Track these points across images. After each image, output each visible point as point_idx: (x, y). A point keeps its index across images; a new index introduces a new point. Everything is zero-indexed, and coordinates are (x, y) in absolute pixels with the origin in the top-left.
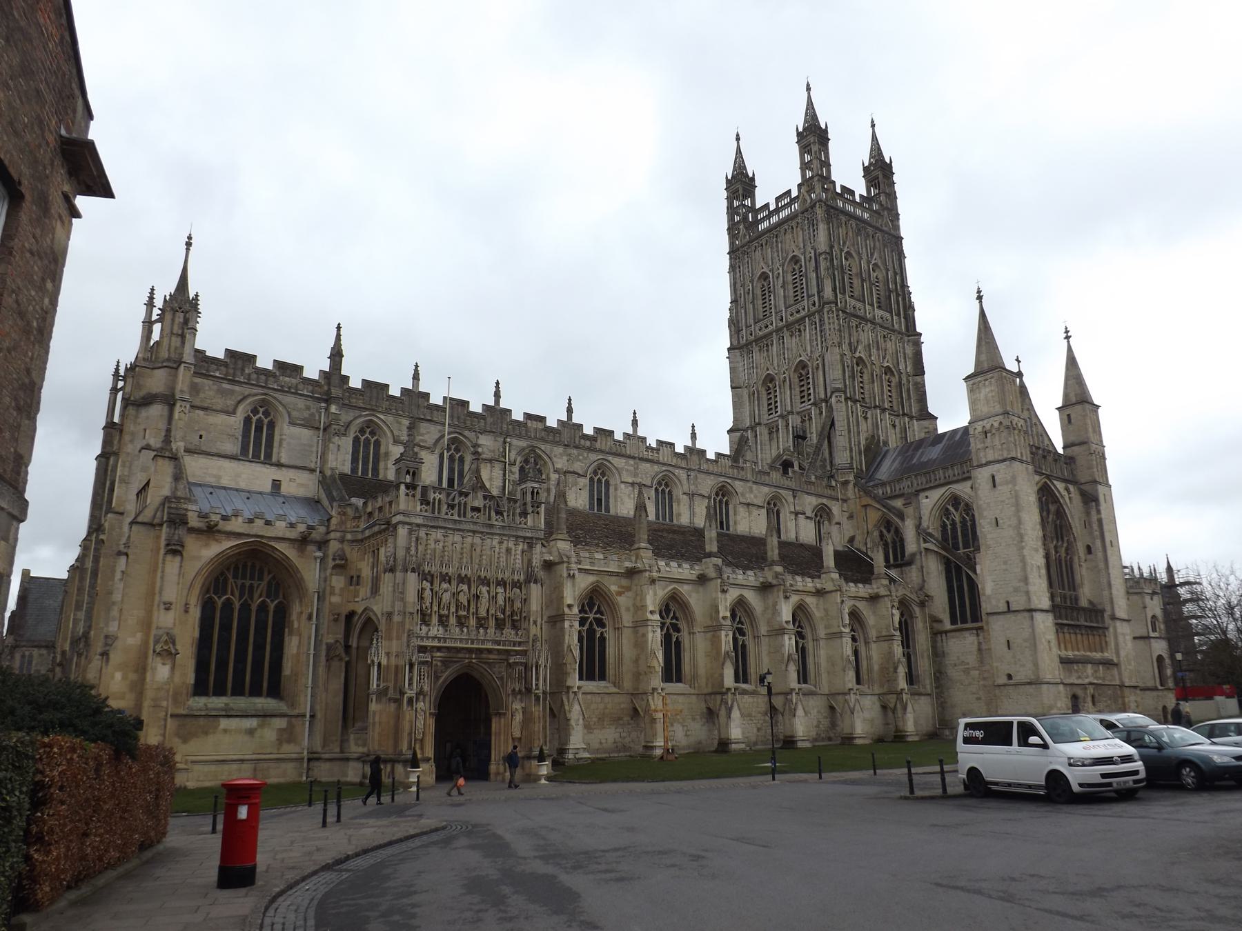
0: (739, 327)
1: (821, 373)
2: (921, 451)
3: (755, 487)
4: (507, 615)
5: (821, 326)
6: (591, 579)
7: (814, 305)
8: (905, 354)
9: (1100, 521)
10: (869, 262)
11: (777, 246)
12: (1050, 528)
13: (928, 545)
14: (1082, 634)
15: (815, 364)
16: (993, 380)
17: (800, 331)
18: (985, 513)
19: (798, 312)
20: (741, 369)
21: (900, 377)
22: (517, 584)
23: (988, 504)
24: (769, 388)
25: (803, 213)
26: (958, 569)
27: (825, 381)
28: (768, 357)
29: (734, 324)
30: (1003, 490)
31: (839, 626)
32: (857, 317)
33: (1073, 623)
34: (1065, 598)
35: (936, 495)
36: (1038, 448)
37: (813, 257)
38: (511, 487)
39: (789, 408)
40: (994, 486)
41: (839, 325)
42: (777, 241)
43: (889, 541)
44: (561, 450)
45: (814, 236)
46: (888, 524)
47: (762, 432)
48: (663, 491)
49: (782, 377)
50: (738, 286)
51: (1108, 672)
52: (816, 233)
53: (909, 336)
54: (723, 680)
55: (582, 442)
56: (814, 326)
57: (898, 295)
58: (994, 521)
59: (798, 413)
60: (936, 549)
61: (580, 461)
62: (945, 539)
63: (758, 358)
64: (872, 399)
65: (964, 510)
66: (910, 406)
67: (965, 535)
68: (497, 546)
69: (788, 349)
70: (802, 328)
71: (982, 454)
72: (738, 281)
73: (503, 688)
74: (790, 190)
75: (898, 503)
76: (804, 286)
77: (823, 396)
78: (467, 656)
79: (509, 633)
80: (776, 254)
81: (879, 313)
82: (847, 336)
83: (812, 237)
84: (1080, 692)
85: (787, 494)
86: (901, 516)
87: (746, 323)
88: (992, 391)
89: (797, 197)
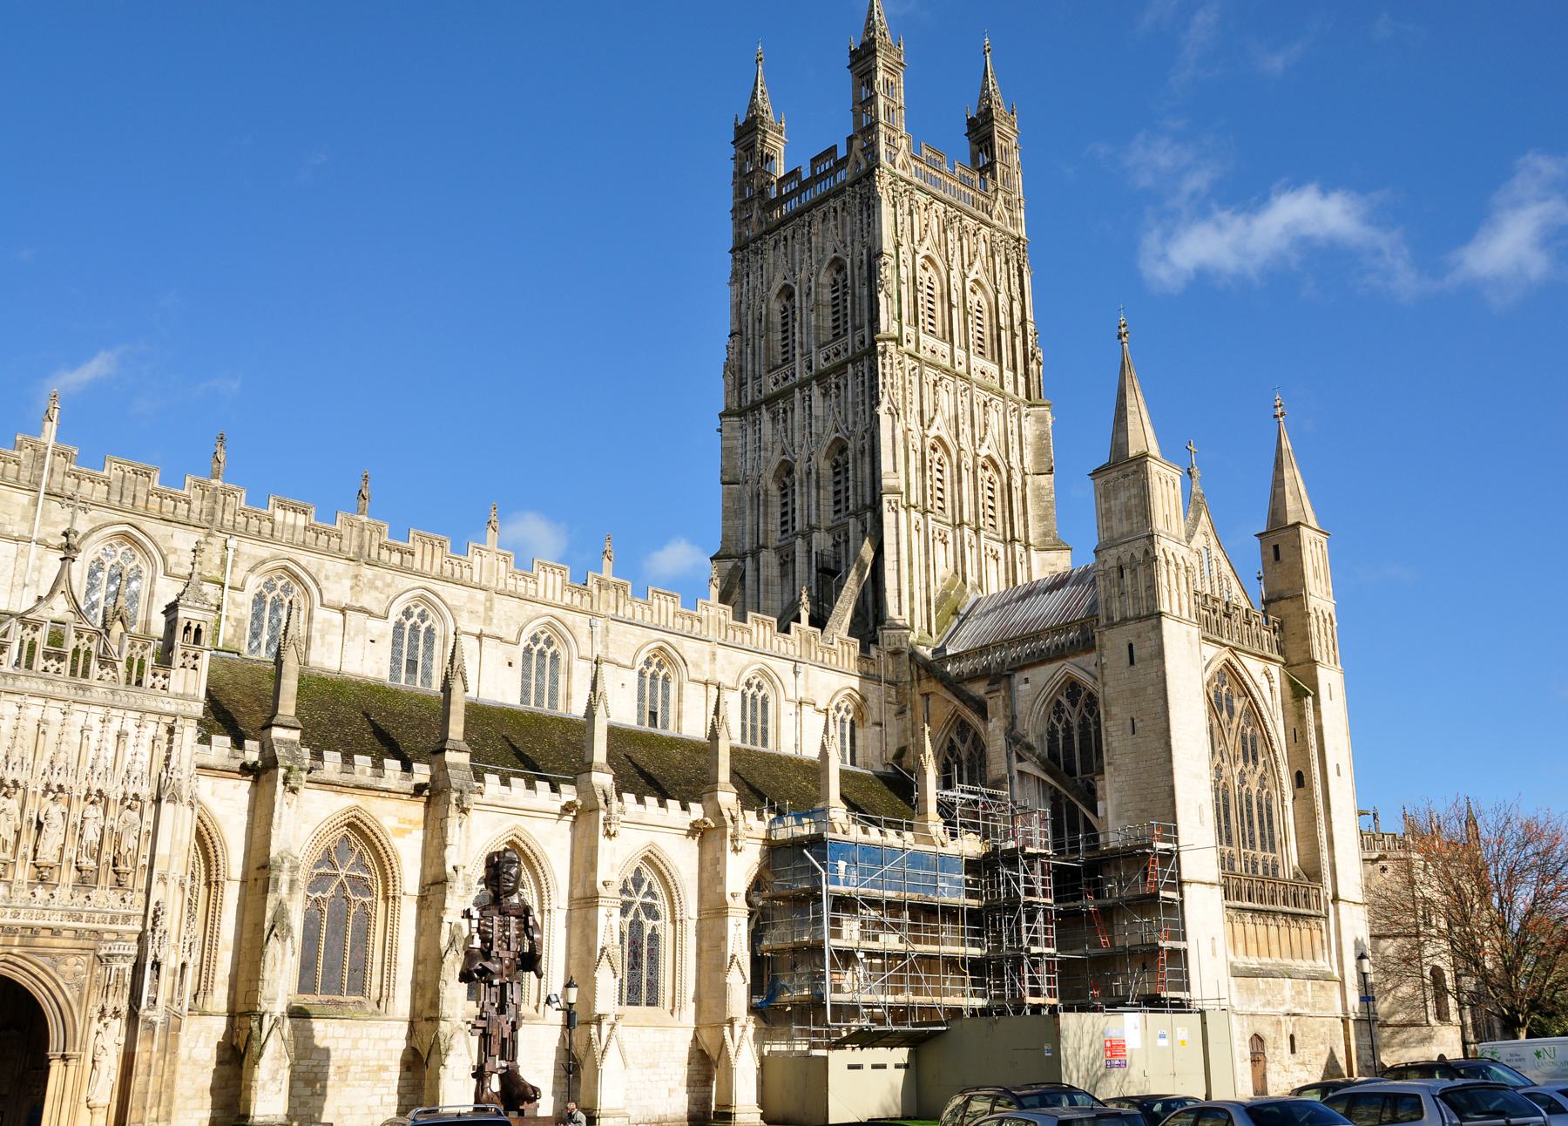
1: (867, 459)
3: (720, 651)
4: (103, 860)
6: (346, 801)
7: (862, 343)
8: (1020, 436)
9: (1319, 730)
10: (965, 276)
12: (1233, 741)
14: (1278, 926)
17: (838, 387)
18: (1115, 710)
19: (837, 354)
20: (740, 451)
22: (130, 802)
24: (785, 486)
25: (852, 185)
26: (1073, 810)
32: (936, 366)
33: (1261, 907)
34: (1255, 864)
36: (1214, 600)
37: (865, 262)
38: (231, 631)
40: (1132, 662)
41: (903, 378)
42: (809, 232)
43: (963, 758)
44: (340, 566)
46: (963, 727)
47: (769, 559)
48: (541, 654)
50: (743, 306)
51: (1323, 994)
53: (1030, 406)
55: (385, 554)
56: (860, 379)
57: (1014, 336)
61: (377, 588)
62: (1053, 755)
66: (1026, 526)
68: (97, 727)
72: (744, 299)
73: (80, 1004)
74: (835, 147)
75: (979, 689)
76: (849, 311)
77: (868, 501)
79: (104, 897)
81: (977, 362)
82: (916, 397)
83: (865, 226)
84: (1267, 1031)
85: (783, 669)
86: (981, 709)
89: (845, 159)
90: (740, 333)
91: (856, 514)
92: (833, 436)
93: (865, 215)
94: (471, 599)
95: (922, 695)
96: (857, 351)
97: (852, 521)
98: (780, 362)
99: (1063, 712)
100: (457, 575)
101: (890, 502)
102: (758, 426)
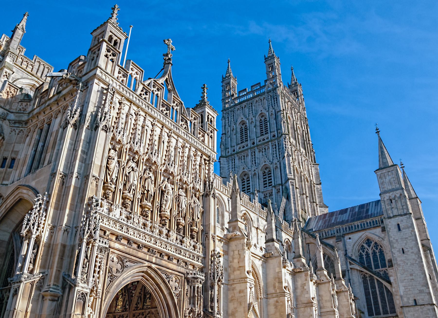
0: (226, 147)
1: (279, 170)
2: (334, 217)
5: (279, 146)
11: (252, 109)
15: (275, 166)
16: (393, 172)
17: (265, 149)
20: (226, 168)
21: (311, 183)
23: (397, 240)
24: (243, 179)
28: (245, 162)
29: (224, 145)
30: (406, 232)
31: (332, 307)
35: (356, 237)
40: (399, 229)
45: (274, 103)
49: (253, 173)
52: (275, 102)
58: (401, 249)
59: (263, 192)
60: (359, 268)
65: (374, 246)
66: (316, 199)
67: (375, 260)
69: (257, 158)
70: (266, 148)
71: (389, 212)
72: (227, 124)
75: (331, 242)
77: (280, 183)
80: (251, 112)
87: (231, 145)
88: (393, 178)
90: (225, 134)
91: (275, 186)
92: (264, 164)
95: (307, 244)
96: (272, 139)
97: (274, 189)
98: (240, 143)
99: (365, 248)
101: (291, 182)
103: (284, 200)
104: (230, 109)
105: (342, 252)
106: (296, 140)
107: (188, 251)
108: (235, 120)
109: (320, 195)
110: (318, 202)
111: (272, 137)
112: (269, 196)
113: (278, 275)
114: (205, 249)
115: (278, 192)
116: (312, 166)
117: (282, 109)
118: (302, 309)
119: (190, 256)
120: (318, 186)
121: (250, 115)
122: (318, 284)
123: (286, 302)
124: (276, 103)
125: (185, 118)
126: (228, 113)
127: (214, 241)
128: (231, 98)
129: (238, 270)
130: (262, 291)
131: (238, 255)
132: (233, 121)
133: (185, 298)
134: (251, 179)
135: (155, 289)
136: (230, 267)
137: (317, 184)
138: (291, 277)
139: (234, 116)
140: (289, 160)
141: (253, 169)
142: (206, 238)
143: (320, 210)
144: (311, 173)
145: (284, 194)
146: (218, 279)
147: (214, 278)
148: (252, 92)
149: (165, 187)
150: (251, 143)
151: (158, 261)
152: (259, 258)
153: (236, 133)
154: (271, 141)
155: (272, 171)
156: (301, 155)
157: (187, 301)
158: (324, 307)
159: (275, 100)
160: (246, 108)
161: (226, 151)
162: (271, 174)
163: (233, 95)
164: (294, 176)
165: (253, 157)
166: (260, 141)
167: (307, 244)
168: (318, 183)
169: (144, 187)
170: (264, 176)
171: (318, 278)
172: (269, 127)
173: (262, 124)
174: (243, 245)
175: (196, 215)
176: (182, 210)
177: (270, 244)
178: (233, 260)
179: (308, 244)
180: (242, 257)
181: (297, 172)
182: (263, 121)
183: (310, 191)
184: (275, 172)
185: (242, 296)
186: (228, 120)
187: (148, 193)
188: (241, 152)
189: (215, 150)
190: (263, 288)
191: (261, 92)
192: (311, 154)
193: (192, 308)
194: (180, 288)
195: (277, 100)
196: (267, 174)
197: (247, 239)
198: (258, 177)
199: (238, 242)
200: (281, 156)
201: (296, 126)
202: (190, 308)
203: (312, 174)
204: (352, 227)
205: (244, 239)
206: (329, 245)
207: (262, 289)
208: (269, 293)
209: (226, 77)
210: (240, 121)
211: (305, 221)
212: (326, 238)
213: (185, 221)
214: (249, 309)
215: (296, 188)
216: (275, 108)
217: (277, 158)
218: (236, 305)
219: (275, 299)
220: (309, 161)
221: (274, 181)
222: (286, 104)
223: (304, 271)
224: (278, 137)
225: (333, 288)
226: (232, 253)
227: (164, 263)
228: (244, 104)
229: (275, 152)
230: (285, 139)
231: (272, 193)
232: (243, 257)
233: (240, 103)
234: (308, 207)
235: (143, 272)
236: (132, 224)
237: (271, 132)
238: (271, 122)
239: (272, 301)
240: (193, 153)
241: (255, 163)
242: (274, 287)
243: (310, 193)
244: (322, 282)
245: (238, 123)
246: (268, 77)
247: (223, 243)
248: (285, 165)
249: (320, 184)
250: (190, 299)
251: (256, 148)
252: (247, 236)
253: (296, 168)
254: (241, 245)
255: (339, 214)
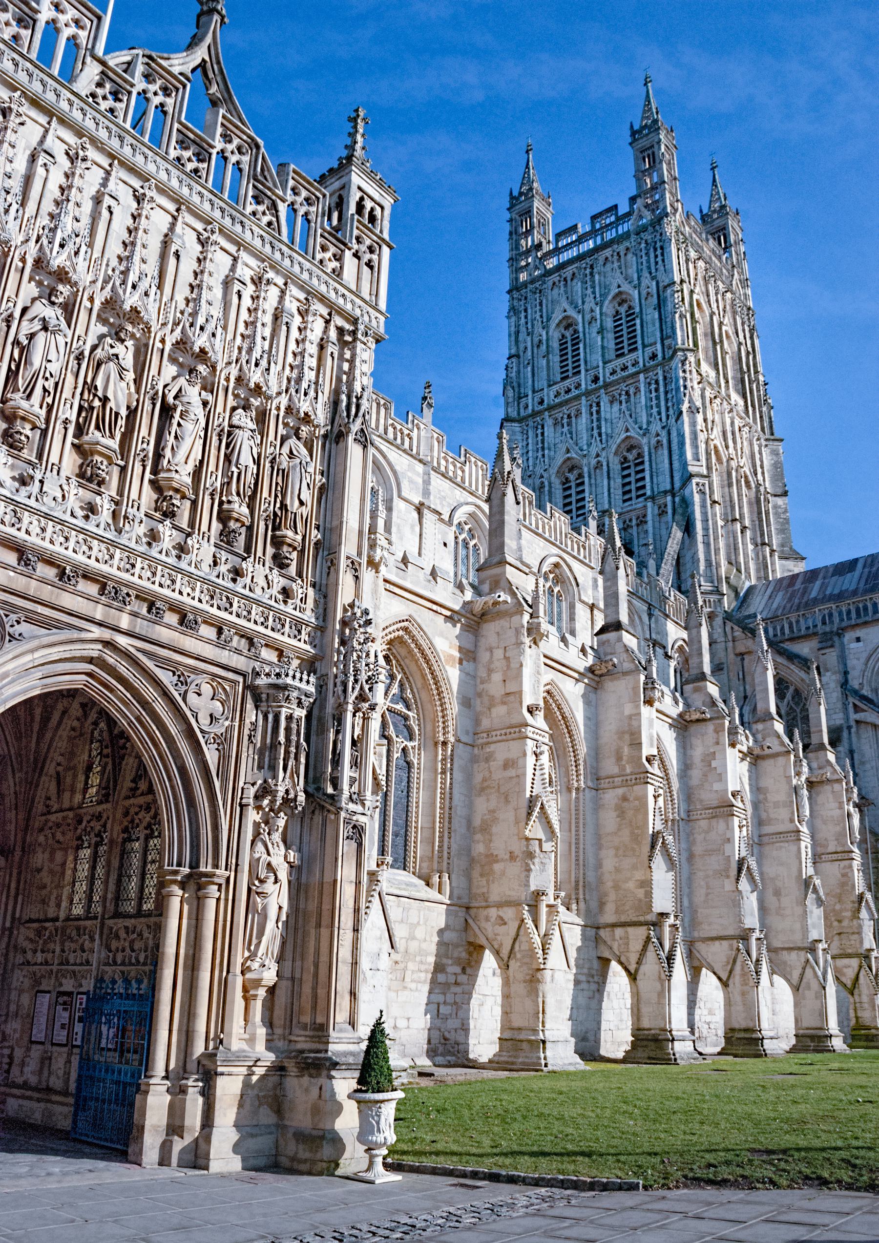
0: (519, 393)
1: (666, 452)
2: (818, 583)
5: (666, 385)
13: (860, 716)
15: (654, 441)
17: (627, 393)
21: (758, 491)
24: (567, 480)
27: (671, 464)
28: (571, 433)
29: (513, 388)
39: (606, 507)
45: (657, 263)
49: (593, 462)
52: (659, 259)
54: (649, 894)
63: (552, 435)
64: (729, 508)
66: (770, 536)
69: (606, 420)
70: (632, 391)
72: (523, 329)
75: (805, 649)
77: (668, 487)
78: (99, 613)
80: (589, 291)
90: (518, 356)
91: (653, 498)
92: (623, 436)
93: (652, 255)
94: (411, 468)
95: (737, 655)
97: (649, 504)
100: (399, 441)
101: (697, 484)
102: (539, 431)
103: (677, 534)
104: (530, 287)
105: (834, 677)
106: (718, 370)
107: (258, 602)
108: (544, 315)
109: (782, 524)
110: (778, 546)
111: (647, 359)
112: (638, 525)
113: (630, 725)
114: (326, 603)
115: (662, 513)
116: (764, 443)
117: (677, 279)
118: (703, 824)
119: (267, 619)
120: (780, 501)
121: (587, 299)
122: (755, 758)
123: (651, 800)
124: (660, 262)
125: (269, 193)
126: (526, 298)
127: (357, 577)
128: (533, 253)
129: (504, 703)
130: (581, 767)
131: (504, 662)
132: (538, 318)
133: (245, 749)
134: (586, 480)
135: (138, 719)
136: (479, 695)
137: (775, 496)
138: (674, 735)
139: (541, 304)
140: (693, 424)
141: (594, 451)
142: (329, 568)
143: (782, 566)
144: (758, 463)
145: (676, 517)
146: (356, 693)
147: (345, 691)
148: (593, 233)
149: (176, 398)
150: (589, 379)
151: (141, 626)
152: (576, 675)
153: (548, 353)
154: (646, 370)
155: (646, 454)
156: (731, 411)
157: (250, 760)
158: (769, 821)
159: (659, 252)
160: (575, 281)
161: (519, 404)
162: (642, 463)
163: (539, 246)
164: (709, 468)
165: (595, 416)
166: (613, 372)
167: (737, 655)
168: (779, 491)
169: (91, 387)
170: (623, 469)
171: (755, 741)
172: (639, 332)
173: (621, 325)
174: (518, 632)
175: (292, 493)
176: (239, 474)
177: (611, 636)
178: (489, 675)
179: (742, 654)
180: (514, 665)
181: (719, 459)
182: (623, 316)
183: (756, 515)
184: (653, 458)
185: (511, 778)
186: (526, 317)
187: (104, 406)
188: (561, 405)
189: (383, 305)
190: (585, 761)
191: (620, 232)
192: (761, 412)
193: (265, 781)
194: (227, 719)
195: (662, 255)
196: (631, 464)
197: (531, 615)
198: (605, 474)
199: (503, 623)
200: (671, 412)
201: (720, 329)
202: (260, 782)
203: (762, 467)
204: (866, 608)
205: (521, 612)
206: (798, 656)
207: (581, 762)
208: (603, 774)
209: (521, 194)
210: (560, 317)
211: (737, 593)
212: (791, 639)
213: (251, 507)
214: (529, 814)
215: (715, 502)
216: (659, 278)
217: (661, 419)
218: (493, 804)
219: (620, 791)
220: (753, 429)
221: (652, 482)
222: (691, 266)
223: (710, 719)
224: (664, 358)
225: (798, 769)
226: (488, 654)
227: (163, 634)
228: (571, 269)
229: (654, 402)
230: (683, 363)
231: (645, 516)
232: (518, 666)
233: (561, 267)
234: (746, 555)
235: (91, 660)
236: (33, 499)
237: (644, 346)
238: (648, 318)
239: (611, 797)
240: (298, 304)
241: (600, 435)
242: (619, 758)
243: (756, 519)
244: (767, 751)
245: (553, 325)
246: (639, 187)
247: (459, 625)
248: (681, 436)
249: (785, 494)
250: (261, 753)
251: (602, 391)
252: (531, 607)
253: (715, 447)
254: (511, 633)
255: (833, 576)
